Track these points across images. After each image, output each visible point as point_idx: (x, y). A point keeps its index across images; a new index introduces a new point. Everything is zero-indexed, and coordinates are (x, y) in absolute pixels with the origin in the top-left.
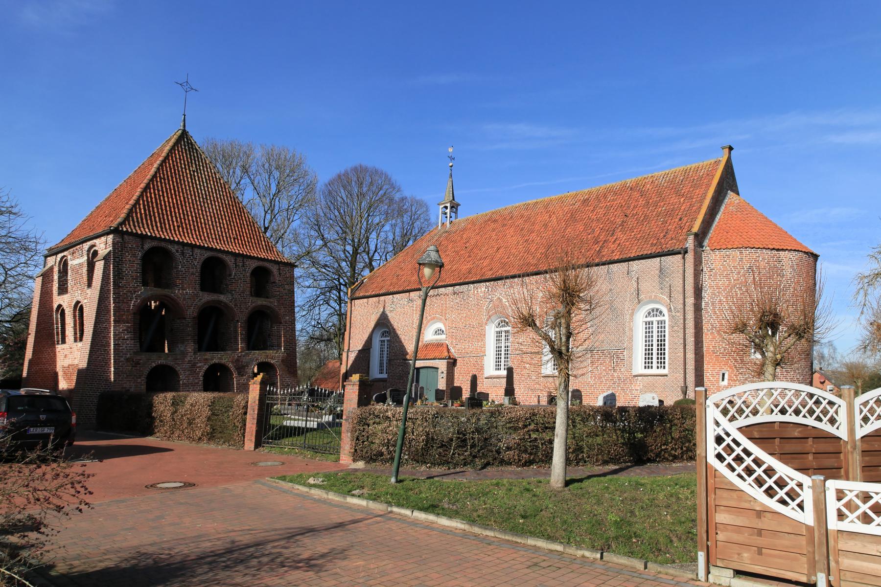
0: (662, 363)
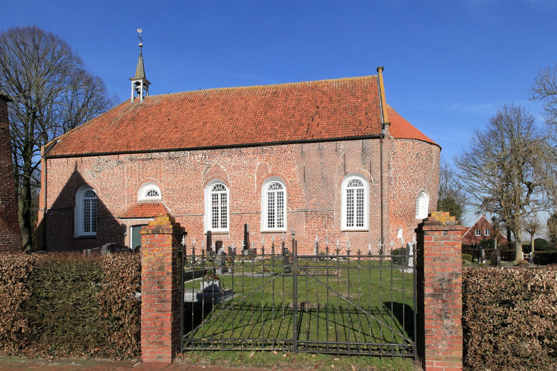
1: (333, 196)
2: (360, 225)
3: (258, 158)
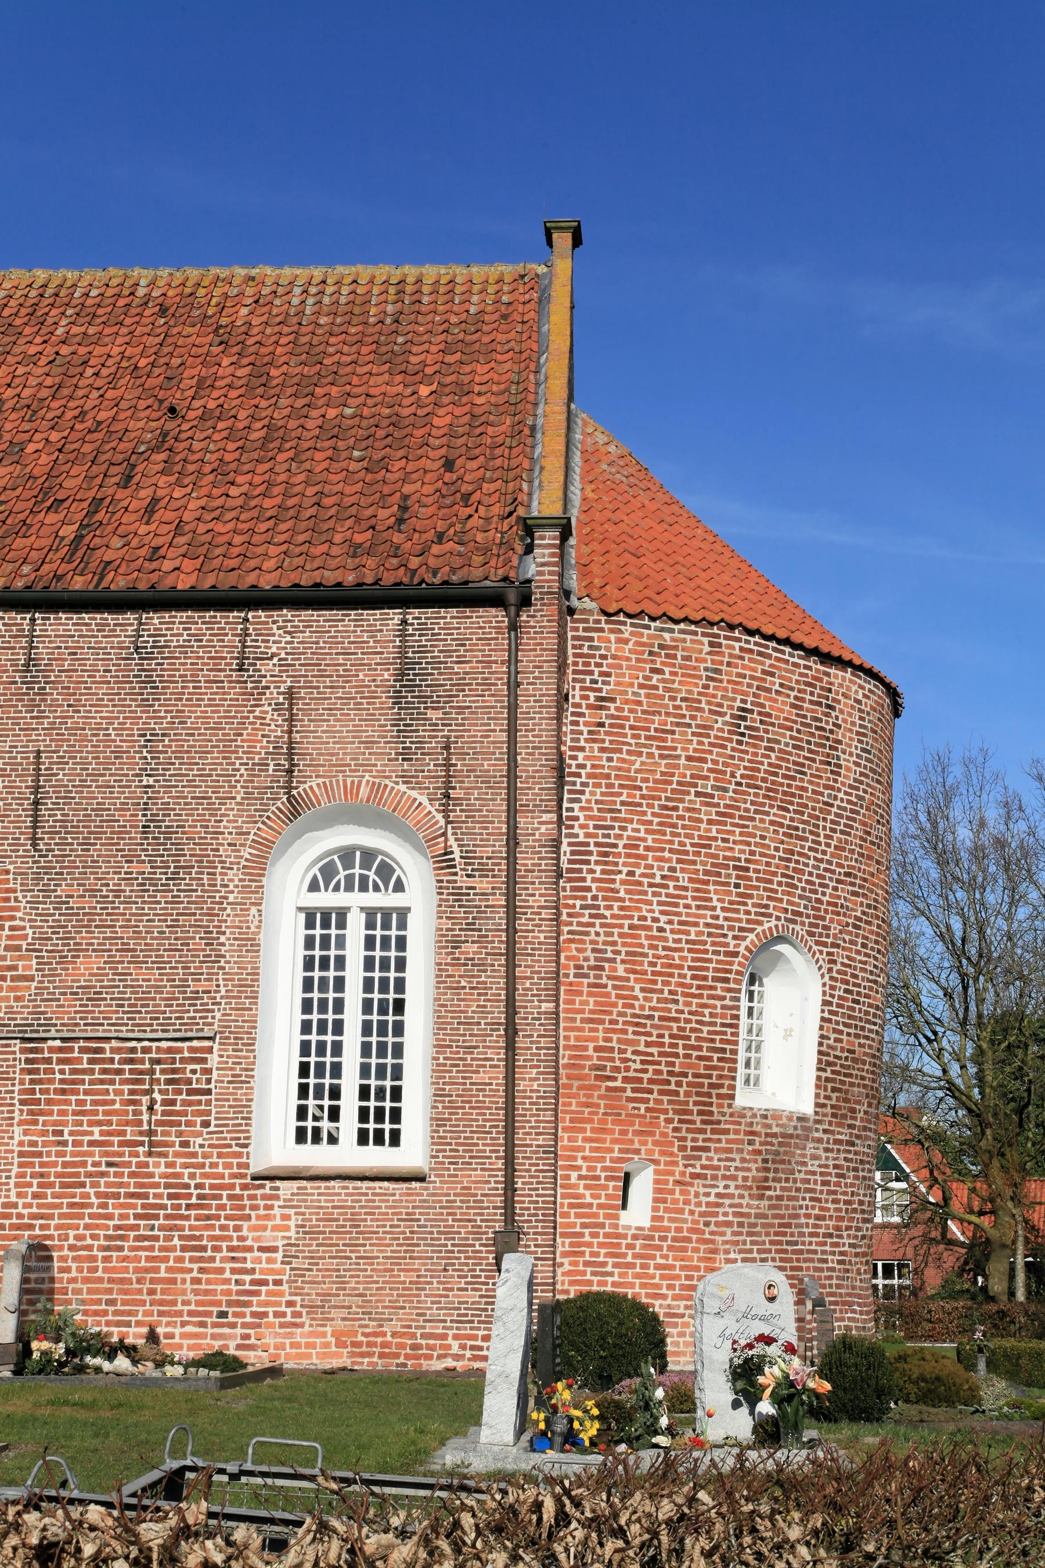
0: (381, 1124)
1: (210, 946)
2: (379, 1140)
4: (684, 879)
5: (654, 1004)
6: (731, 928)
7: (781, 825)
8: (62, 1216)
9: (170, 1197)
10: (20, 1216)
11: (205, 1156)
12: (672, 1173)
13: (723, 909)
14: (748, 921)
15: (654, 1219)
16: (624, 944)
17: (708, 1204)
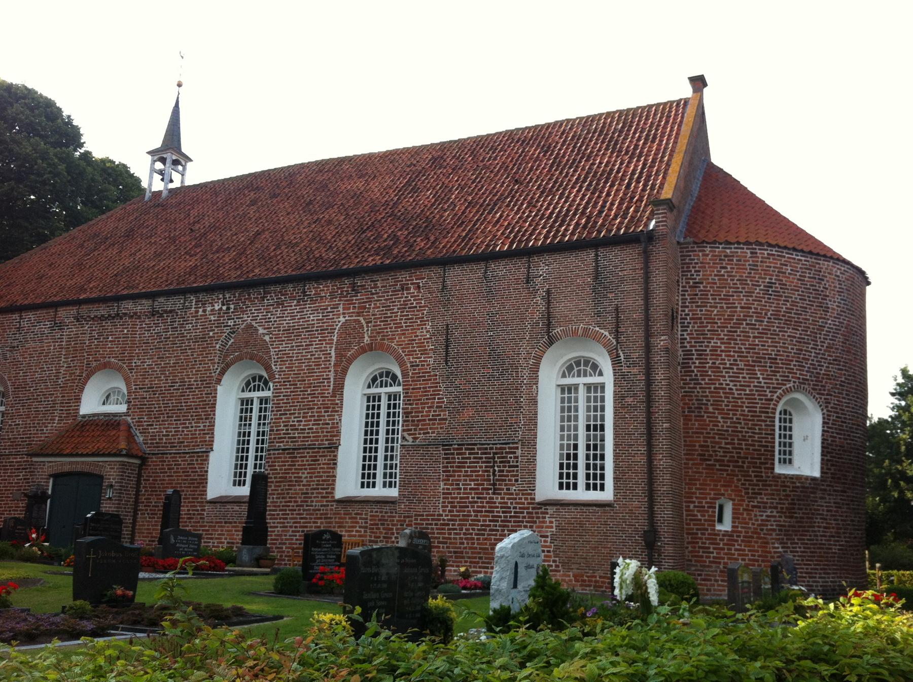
0: (595, 481)
2: (595, 489)
3: (341, 309)
4: (741, 365)
5: (729, 424)
6: (768, 387)
7: (795, 337)
8: (460, 520)
9: (503, 512)
10: (444, 520)
11: (517, 494)
12: (742, 505)
13: (763, 379)
14: (778, 384)
15: (733, 527)
16: (712, 397)
17: (762, 520)
